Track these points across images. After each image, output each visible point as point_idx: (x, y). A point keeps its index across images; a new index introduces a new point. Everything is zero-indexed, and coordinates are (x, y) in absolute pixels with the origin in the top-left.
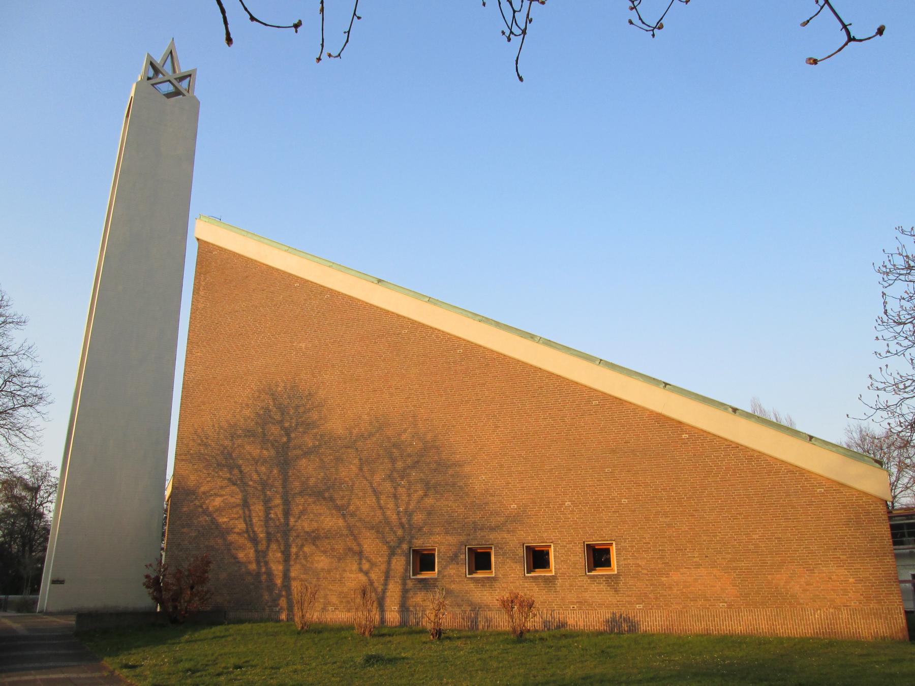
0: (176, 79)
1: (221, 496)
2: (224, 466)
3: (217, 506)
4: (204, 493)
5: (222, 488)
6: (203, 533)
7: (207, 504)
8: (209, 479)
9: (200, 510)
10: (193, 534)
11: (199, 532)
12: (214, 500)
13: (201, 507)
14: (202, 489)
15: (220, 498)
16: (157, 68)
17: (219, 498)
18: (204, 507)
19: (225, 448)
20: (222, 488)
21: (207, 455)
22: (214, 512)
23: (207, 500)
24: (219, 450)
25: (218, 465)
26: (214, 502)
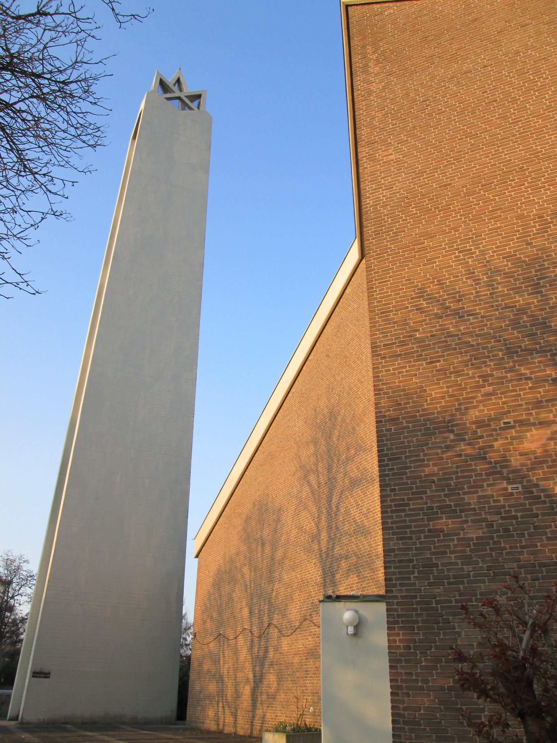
0: (187, 97)
1: (543, 424)
2: (530, 352)
3: (534, 452)
4: (480, 424)
5: (538, 404)
6: (507, 530)
7: (498, 451)
8: (490, 389)
9: (480, 467)
10: (473, 534)
11: (490, 526)
12: (519, 437)
13: (482, 457)
14: (474, 414)
15: (541, 431)
16: (168, 86)
17: (534, 432)
18: (493, 456)
19: (522, 311)
20: (538, 404)
21: (470, 334)
22: (532, 469)
23: (496, 440)
24: (501, 318)
25: (510, 352)
26: (521, 443)
